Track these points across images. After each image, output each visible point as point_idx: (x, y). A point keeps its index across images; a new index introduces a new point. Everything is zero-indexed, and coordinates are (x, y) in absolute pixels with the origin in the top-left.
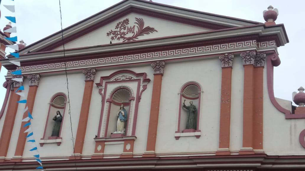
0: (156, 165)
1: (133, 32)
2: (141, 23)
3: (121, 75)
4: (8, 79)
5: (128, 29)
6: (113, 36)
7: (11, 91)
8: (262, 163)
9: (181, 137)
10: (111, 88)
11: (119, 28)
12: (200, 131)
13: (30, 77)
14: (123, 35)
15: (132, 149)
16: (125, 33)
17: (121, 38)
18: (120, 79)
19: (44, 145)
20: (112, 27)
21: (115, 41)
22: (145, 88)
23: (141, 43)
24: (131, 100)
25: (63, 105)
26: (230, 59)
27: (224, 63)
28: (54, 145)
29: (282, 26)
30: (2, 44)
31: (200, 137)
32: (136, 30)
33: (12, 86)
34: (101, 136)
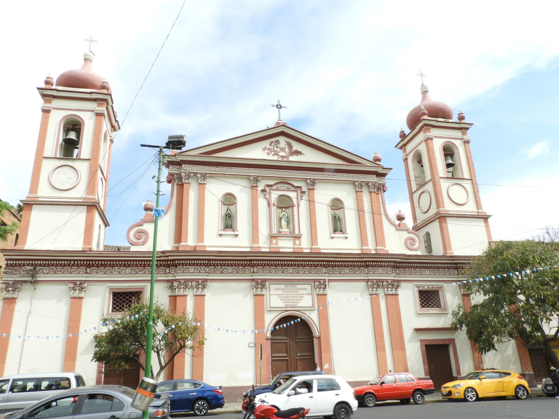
0: (335, 258)
1: (285, 152)
2: (290, 146)
4: (170, 174)
5: (280, 148)
6: (269, 152)
7: (177, 184)
8: (402, 259)
10: (274, 195)
11: (272, 146)
12: (347, 234)
15: (300, 244)
19: (222, 236)
20: (266, 143)
21: (271, 157)
23: (299, 163)
24: (293, 207)
28: (232, 236)
29: (391, 169)
30: (112, 129)
32: (287, 150)
33: (177, 180)
34: (273, 233)
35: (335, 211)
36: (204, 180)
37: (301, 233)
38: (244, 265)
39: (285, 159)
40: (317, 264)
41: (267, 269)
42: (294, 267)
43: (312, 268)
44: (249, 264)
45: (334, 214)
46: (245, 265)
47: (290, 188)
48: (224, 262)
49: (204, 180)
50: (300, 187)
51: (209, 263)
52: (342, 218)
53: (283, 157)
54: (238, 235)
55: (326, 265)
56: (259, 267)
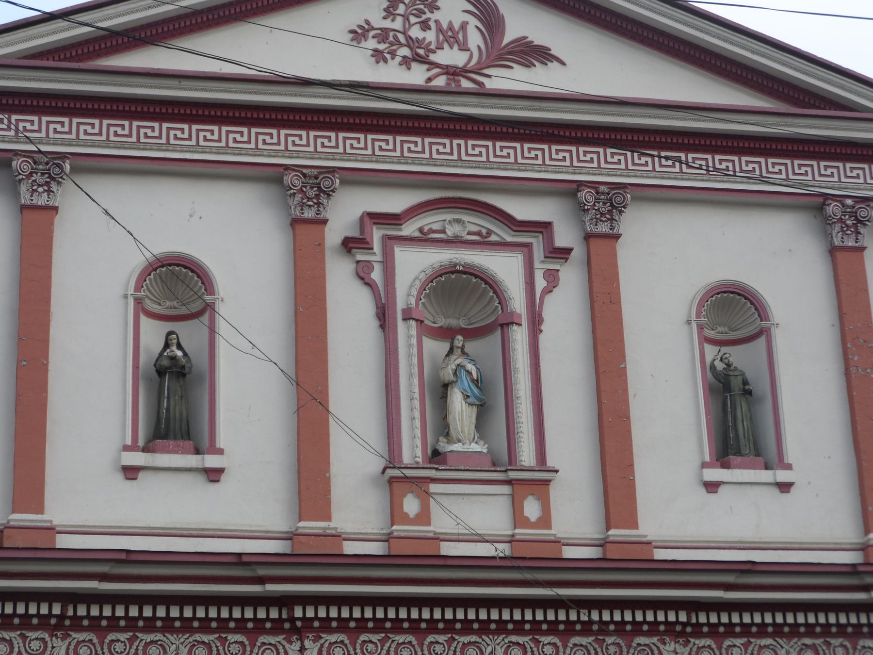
0: (728, 587)
1: (464, 48)
3: (449, 217)
5: (440, 29)
6: (382, 47)
9: (724, 483)
11: (399, 20)
12: (789, 467)
13: (27, 168)
14: (421, 52)
15: (545, 521)
16: (430, 43)
17: (415, 60)
18: (443, 231)
19: (141, 475)
22: (552, 278)
23: (536, 104)
25: (175, 303)
26: (859, 221)
27: (843, 231)
31: (793, 489)
32: (475, 39)
34: (407, 459)
35: (724, 349)
36: (49, 191)
37: (550, 463)
38: (250, 625)
39: (465, 84)
40: (634, 622)
41: (370, 647)
42: (514, 638)
43: (610, 640)
44: (280, 620)
45: (720, 366)
46: (259, 626)
47: (490, 232)
48: (148, 612)
49: (49, 191)
50: (544, 228)
51: (70, 613)
52: (760, 384)
53: (454, 74)
54: (220, 471)
55: (678, 628)
56: (333, 638)
